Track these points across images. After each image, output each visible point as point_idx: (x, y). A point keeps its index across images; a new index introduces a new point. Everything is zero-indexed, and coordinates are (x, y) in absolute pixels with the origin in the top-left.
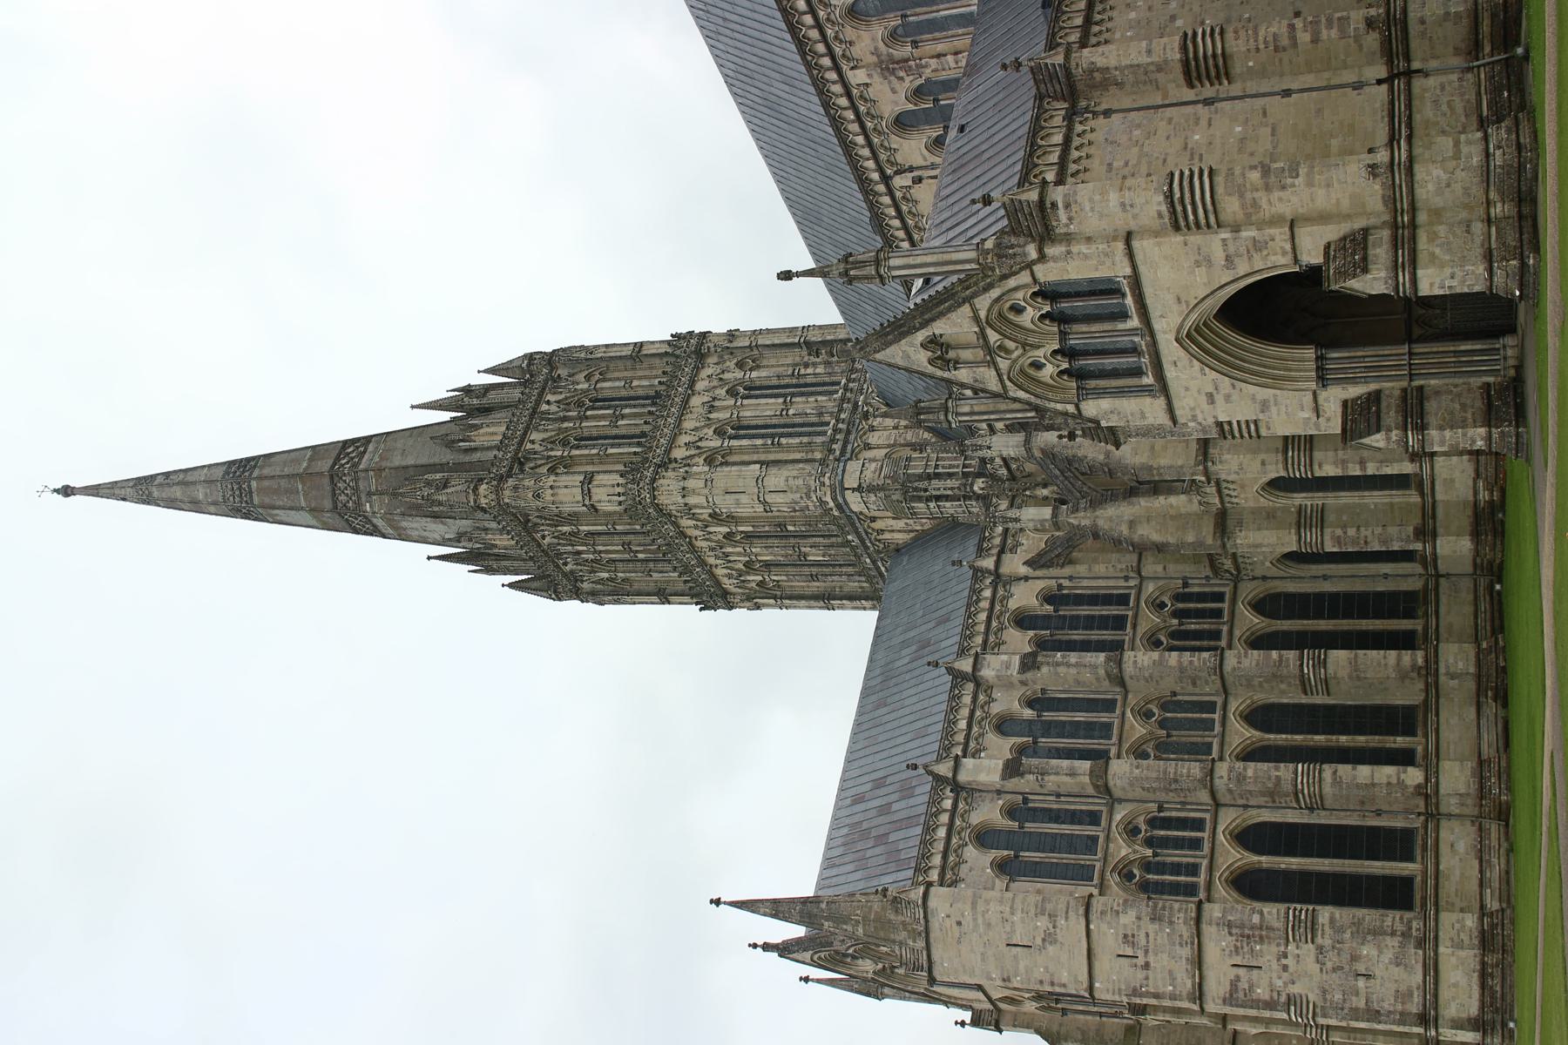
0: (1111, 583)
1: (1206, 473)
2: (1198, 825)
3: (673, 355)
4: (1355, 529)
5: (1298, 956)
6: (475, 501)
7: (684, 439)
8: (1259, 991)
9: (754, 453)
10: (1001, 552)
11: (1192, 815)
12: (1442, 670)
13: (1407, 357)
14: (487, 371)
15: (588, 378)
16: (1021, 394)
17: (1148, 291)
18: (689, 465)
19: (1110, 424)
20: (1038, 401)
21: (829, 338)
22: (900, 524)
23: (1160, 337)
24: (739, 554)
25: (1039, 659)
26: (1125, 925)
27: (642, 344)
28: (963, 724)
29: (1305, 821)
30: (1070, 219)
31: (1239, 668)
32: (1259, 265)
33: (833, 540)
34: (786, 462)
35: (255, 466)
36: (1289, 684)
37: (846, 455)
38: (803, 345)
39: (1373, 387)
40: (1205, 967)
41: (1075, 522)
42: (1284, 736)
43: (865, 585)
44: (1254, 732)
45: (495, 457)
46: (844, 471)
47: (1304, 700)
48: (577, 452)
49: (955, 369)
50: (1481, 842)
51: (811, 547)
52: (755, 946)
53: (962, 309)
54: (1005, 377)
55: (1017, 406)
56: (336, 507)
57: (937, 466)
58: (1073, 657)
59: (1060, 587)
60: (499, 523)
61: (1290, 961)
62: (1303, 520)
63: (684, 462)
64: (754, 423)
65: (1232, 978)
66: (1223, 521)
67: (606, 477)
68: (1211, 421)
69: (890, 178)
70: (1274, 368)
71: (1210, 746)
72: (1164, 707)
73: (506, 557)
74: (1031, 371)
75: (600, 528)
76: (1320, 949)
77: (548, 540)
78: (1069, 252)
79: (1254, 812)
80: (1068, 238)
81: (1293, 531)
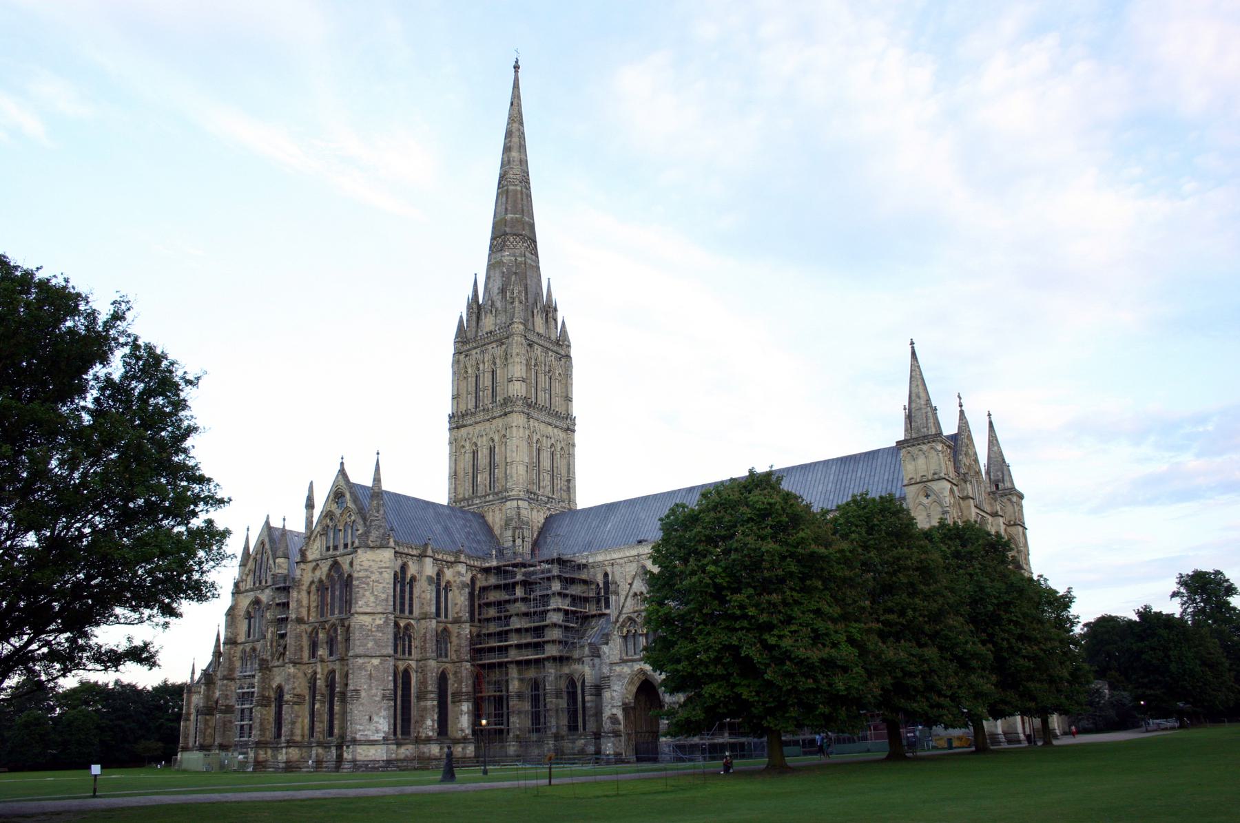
2: (410, 654)
7: (536, 424)
14: (563, 322)
22: (497, 520)
37: (529, 500)
43: (461, 496)
46: (525, 500)
73: (478, 318)
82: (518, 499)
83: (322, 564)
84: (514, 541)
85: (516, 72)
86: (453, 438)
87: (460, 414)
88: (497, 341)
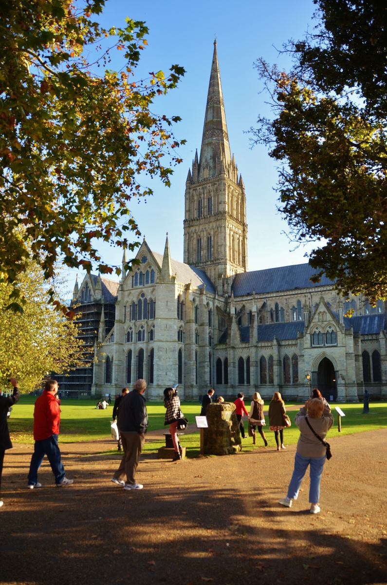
1: (251, 347)
2: (181, 341)
10: (218, 300)
17: (335, 348)
23: (324, 349)
24: (203, 234)
61: (168, 360)
62: (234, 363)
66: (233, 348)
76: (171, 366)
77: (208, 187)
83: (133, 291)
84: (223, 286)
85: (215, 46)
86: (186, 232)
88: (211, 183)
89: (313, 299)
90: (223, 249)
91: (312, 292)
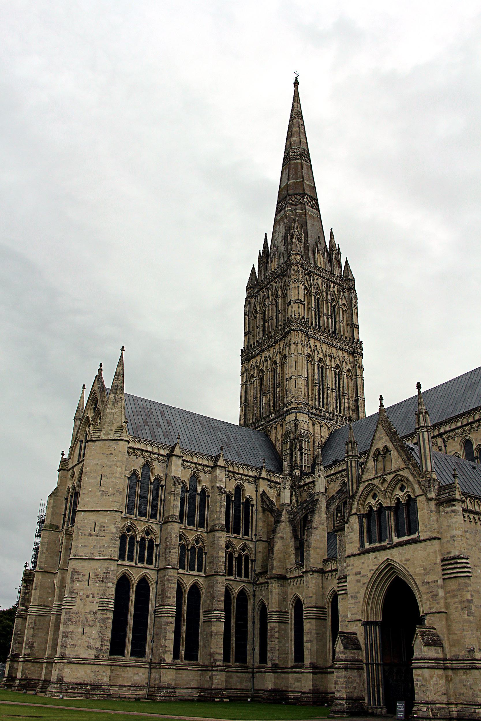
0: (254, 528)
1: (306, 572)
2: (150, 562)
3: (353, 342)
4: (278, 637)
5: (93, 602)
6: (293, 254)
7: (318, 344)
8: (78, 584)
9: (312, 375)
10: (269, 481)
11: (154, 559)
12: (214, 673)
13: (377, 663)
14: (347, 261)
15: (344, 305)
16: (361, 489)
17: (412, 546)
18: (307, 346)
19: (346, 528)
20: (358, 496)
21: (360, 409)
22: (279, 437)
23: (389, 551)
24: (267, 367)
25: (223, 495)
26: (108, 527)
27: (358, 328)
28: (195, 460)
29: (150, 609)
30: (447, 513)
31: (217, 583)
32: (424, 597)
33: (272, 408)
34: (308, 389)
35: (307, 162)
36: (209, 605)
37: (310, 413)
38: (357, 398)
39: (363, 647)
40: (89, 561)
41: (283, 513)
42: (186, 601)
43: (251, 421)
44: (189, 588)
45: (311, 263)
46: (304, 413)
47: (202, 611)
48: (313, 298)
49: (374, 460)
50: (138, 686)
51: (269, 398)
52: (101, 365)
53: (403, 463)
54: (370, 482)
55: (355, 488)
56: (289, 195)
57: (305, 454)
58: (224, 510)
59: (253, 506)
60: (282, 264)
63: (308, 344)
64: (324, 375)
65: (84, 573)
66: (282, 578)
67: (303, 310)
68: (348, 573)
69: (441, 437)
70: (372, 602)
71: (183, 568)
72: (200, 549)
73: (266, 266)
74: (372, 494)
75: (280, 307)
76: (95, 613)
78: (431, 511)
79: (155, 587)
80: (439, 511)
81: (278, 609)
82: (296, 413)
87: (250, 347)
89: (448, 450)
90: (293, 384)
91: (445, 433)
